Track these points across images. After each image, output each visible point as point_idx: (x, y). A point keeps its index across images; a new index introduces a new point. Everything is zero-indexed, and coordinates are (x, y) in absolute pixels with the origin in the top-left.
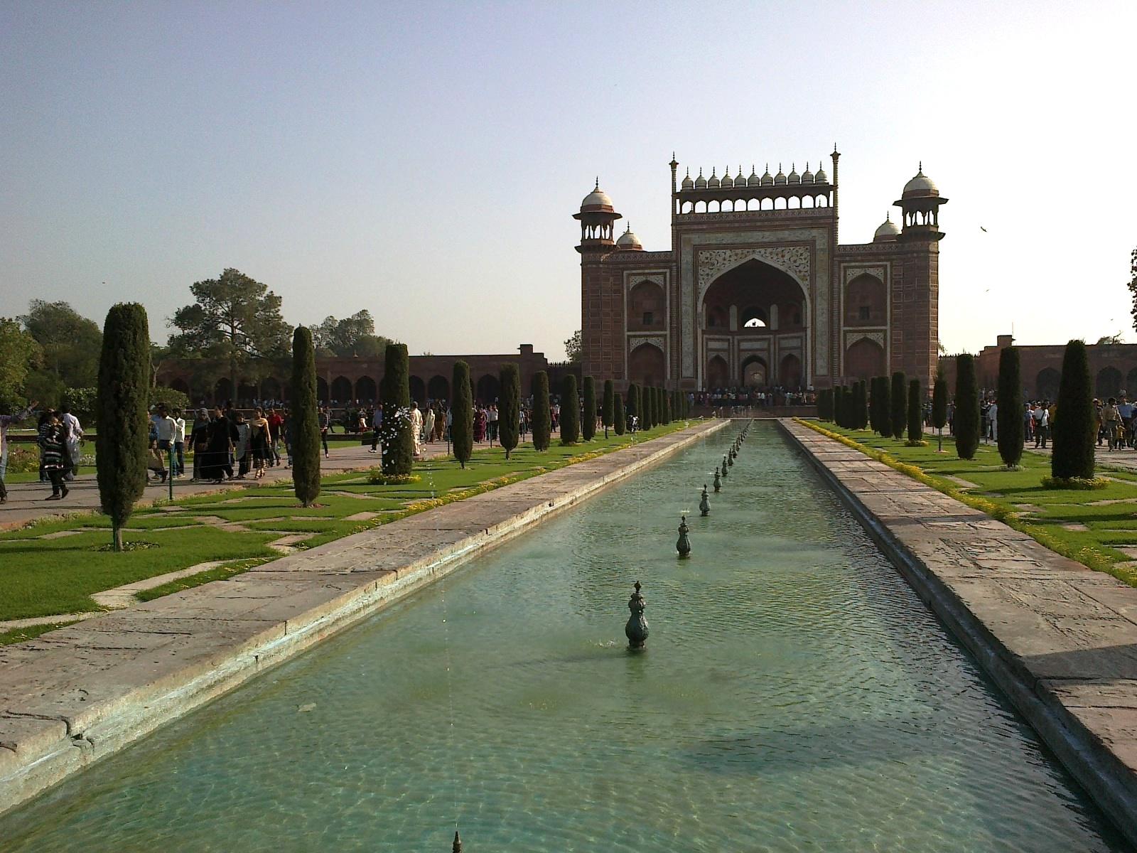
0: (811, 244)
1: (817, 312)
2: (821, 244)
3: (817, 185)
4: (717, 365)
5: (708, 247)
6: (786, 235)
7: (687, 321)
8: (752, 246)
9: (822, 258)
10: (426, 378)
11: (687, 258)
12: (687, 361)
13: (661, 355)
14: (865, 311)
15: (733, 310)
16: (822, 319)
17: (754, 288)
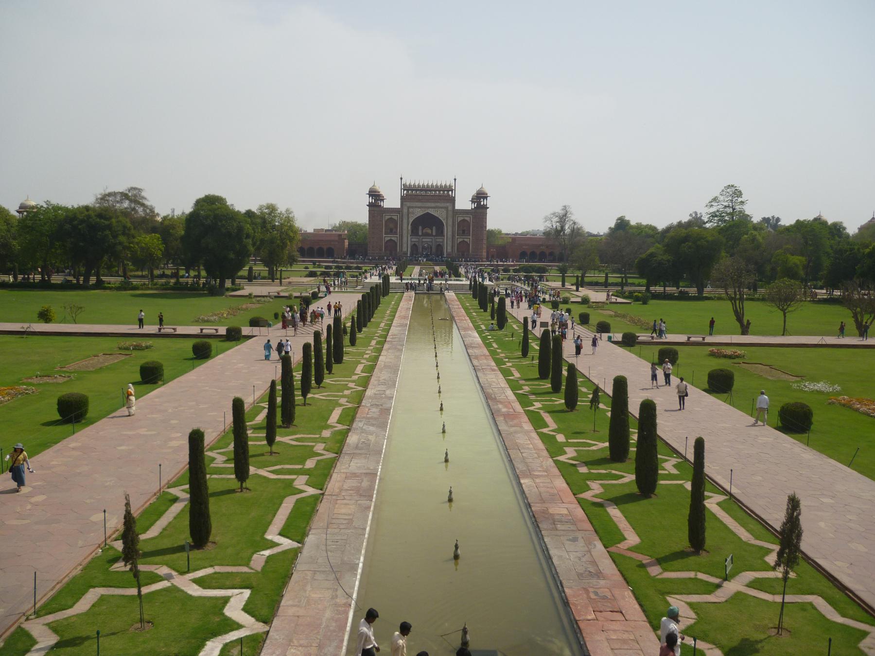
0: (446, 208)
1: (448, 231)
2: (450, 208)
3: (450, 189)
4: (414, 247)
5: (412, 207)
6: (438, 204)
7: (405, 232)
8: (428, 208)
9: (450, 213)
10: (306, 248)
11: (405, 211)
12: (405, 245)
13: (396, 243)
14: (464, 231)
15: (420, 228)
16: (450, 233)
17: (427, 222)
